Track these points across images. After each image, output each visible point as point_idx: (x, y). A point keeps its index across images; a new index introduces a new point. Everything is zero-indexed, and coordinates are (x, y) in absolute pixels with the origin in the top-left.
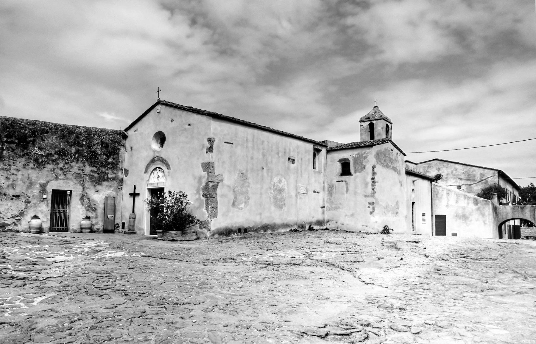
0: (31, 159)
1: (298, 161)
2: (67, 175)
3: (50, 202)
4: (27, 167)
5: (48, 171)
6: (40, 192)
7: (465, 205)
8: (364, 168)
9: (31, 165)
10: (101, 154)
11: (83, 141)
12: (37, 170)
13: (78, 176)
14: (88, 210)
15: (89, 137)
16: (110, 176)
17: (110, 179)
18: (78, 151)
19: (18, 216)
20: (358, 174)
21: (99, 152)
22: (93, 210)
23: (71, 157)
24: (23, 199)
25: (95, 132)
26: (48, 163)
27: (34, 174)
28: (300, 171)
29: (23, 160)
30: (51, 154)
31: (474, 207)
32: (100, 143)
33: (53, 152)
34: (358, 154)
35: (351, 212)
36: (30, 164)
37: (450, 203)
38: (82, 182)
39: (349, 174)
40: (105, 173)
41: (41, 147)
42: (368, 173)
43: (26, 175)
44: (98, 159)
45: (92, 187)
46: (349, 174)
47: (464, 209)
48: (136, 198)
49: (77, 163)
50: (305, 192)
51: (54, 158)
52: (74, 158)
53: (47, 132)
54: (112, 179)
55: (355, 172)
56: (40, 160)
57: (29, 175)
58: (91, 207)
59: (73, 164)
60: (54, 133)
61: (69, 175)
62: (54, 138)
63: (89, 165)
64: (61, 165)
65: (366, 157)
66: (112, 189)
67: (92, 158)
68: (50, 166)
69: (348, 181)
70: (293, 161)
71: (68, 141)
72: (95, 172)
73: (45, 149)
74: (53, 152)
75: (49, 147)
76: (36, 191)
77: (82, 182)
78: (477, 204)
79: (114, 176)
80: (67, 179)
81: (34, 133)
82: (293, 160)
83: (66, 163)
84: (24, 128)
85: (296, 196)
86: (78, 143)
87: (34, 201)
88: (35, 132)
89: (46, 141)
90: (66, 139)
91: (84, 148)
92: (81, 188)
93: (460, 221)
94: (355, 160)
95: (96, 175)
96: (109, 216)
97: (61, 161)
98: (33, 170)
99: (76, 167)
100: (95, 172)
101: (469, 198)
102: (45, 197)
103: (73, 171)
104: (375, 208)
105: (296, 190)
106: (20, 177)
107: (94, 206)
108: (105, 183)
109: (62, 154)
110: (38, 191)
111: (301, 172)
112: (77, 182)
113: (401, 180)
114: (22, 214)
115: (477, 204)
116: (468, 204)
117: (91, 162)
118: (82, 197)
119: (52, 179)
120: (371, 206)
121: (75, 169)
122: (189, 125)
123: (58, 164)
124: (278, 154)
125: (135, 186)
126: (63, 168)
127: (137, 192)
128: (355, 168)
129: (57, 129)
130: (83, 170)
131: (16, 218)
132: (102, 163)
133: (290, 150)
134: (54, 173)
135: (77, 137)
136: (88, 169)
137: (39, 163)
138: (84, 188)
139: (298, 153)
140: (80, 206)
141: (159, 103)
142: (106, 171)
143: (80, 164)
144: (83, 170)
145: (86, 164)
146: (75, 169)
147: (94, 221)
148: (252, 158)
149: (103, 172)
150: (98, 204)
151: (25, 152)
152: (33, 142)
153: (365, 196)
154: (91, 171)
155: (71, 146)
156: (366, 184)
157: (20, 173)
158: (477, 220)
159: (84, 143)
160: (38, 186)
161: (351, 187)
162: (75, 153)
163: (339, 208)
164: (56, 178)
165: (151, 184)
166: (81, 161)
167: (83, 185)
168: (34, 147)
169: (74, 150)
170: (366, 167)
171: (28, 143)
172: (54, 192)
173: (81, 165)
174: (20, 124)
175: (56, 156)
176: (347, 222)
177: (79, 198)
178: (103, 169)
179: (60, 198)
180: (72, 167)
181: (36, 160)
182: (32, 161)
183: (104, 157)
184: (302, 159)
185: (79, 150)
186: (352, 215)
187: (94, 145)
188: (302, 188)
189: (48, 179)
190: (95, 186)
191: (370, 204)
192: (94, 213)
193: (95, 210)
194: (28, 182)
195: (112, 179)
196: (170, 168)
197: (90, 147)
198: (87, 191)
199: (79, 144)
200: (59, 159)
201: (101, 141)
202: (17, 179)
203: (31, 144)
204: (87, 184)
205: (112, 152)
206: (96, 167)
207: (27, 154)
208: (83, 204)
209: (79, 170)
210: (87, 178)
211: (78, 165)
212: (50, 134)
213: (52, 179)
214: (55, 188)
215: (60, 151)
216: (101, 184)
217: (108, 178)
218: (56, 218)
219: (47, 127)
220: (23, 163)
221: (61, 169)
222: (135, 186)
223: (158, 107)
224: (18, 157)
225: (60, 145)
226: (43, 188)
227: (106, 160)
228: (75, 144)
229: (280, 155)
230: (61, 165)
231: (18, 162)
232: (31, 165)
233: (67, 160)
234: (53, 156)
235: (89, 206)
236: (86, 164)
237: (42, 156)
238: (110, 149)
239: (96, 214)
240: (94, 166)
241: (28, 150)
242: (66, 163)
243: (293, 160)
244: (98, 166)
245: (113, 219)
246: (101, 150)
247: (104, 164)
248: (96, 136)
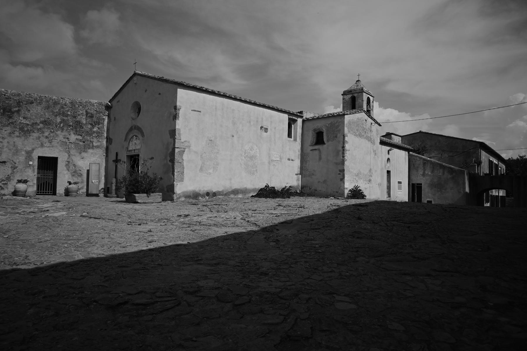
0: (16, 128)
1: (271, 130)
2: (53, 143)
3: (36, 167)
4: (13, 135)
5: (33, 139)
6: (26, 158)
8: (336, 137)
9: (17, 133)
10: (86, 124)
11: (68, 111)
12: (23, 138)
13: (64, 144)
14: (73, 176)
15: (74, 108)
16: (95, 144)
17: (95, 147)
18: (63, 121)
19: (4, 181)
20: (330, 142)
21: (84, 122)
22: (79, 176)
23: (56, 126)
24: (9, 165)
25: (80, 103)
26: (34, 132)
27: (19, 142)
28: (273, 139)
29: (9, 129)
30: (36, 123)
31: (450, 176)
32: (85, 113)
33: (38, 122)
34: (331, 123)
36: (15, 132)
38: (67, 149)
39: (323, 143)
40: (90, 141)
41: (26, 116)
42: (339, 142)
43: (12, 143)
44: (83, 128)
45: (78, 154)
46: (323, 143)
49: (62, 132)
50: (278, 159)
51: (39, 127)
52: (59, 127)
53: (32, 103)
54: (97, 147)
55: (328, 141)
56: (26, 129)
57: (14, 142)
58: (76, 173)
59: (59, 132)
60: (40, 103)
61: (55, 143)
62: (39, 108)
63: (74, 134)
64: (46, 134)
65: (338, 126)
66: (97, 156)
67: (77, 127)
68: (35, 135)
70: (266, 130)
71: (52, 111)
72: (80, 140)
73: (30, 118)
74: (38, 122)
75: (34, 117)
76: (22, 158)
77: (67, 149)
79: (99, 144)
80: (52, 147)
81: (19, 103)
82: (267, 129)
83: (51, 132)
84: (8, 98)
85: (269, 163)
86: (63, 113)
87: (20, 167)
88: (19, 102)
89: (31, 111)
90: (51, 109)
91: (69, 118)
92: (67, 155)
95: (81, 143)
96: (93, 181)
97: (46, 130)
98: (19, 138)
99: (61, 135)
100: (80, 140)
102: (31, 163)
103: (59, 139)
104: (346, 175)
105: (269, 157)
106: (6, 144)
107: (80, 172)
108: (90, 151)
109: (46, 123)
110: (24, 158)
111: (275, 140)
112: (62, 150)
113: (375, 149)
114: (8, 178)
116: (444, 173)
117: (76, 131)
118: (68, 164)
119: (38, 146)
120: (341, 173)
121: (61, 137)
122: (160, 94)
123: (43, 132)
124: (250, 122)
125: (117, 153)
126: (49, 136)
127: (119, 158)
129: (42, 100)
130: (68, 138)
131: (3, 183)
132: (87, 132)
133: (262, 119)
134: (40, 141)
135: (63, 108)
136: (73, 137)
137: (25, 131)
138: (69, 155)
139: (271, 122)
140: (66, 172)
141: (135, 74)
142: (92, 140)
143: (65, 133)
144: (68, 138)
145: (72, 133)
146: (61, 137)
147: (80, 186)
148: (221, 126)
149: (88, 140)
150: (84, 169)
151: (11, 121)
152: (18, 111)
154: (77, 139)
155: (56, 116)
156: (338, 152)
157: (6, 140)
159: (69, 113)
160: (23, 153)
162: (61, 123)
163: (313, 174)
164: (42, 145)
166: (67, 130)
167: (68, 153)
168: (19, 116)
169: (59, 120)
171: (13, 113)
172: (39, 158)
173: (66, 134)
174: (5, 95)
175: (41, 125)
177: (64, 164)
178: (89, 138)
179: (48, 165)
180: (57, 135)
181: (22, 129)
182: (18, 130)
183: (90, 126)
184: (275, 128)
185: (64, 120)
186: (325, 182)
187: (79, 115)
188: (275, 156)
189: (33, 146)
190: (80, 153)
191: (340, 171)
192: (80, 179)
193: (81, 175)
194: (14, 148)
195: (97, 147)
197: (75, 117)
198: (74, 158)
199: (64, 114)
200: (44, 128)
201: (86, 111)
202: (3, 146)
203: (15, 114)
204: (73, 152)
205: (97, 122)
206: (81, 135)
207: (12, 123)
208: (68, 170)
209: (64, 138)
210: (73, 146)
211: (63, 134)
212: (34, 104)
213: (38, 146)
214: (41, 155)
215: (45, 121)
216: (86, 152)
217: (93, 146)
218: (44, 183)
219: (32, 98)
220: (8, 131)
221: (47, 137)
223: (135, 78)
224: (3, 126)
225: (45, 114)
226: (29, 154)
227: (91, 129)
228: (60, 114)
229: (252, 123)
230: (46, 134)
231: (4, 131)
232: (17, 133)
233: (53, 129)
234: (39, 125)
235: (75, 172)
236: (72, 133)
237: (28, 125)
238: (95, 119)
239: (82, 180)
240: (79, 135)
241: (13, 119)
242: (51, 132)
243: (267, 129)
244: (83, 134)
245: (97, 183)
246: (86, 120)
247: (90, 133)
248: (81, 107)
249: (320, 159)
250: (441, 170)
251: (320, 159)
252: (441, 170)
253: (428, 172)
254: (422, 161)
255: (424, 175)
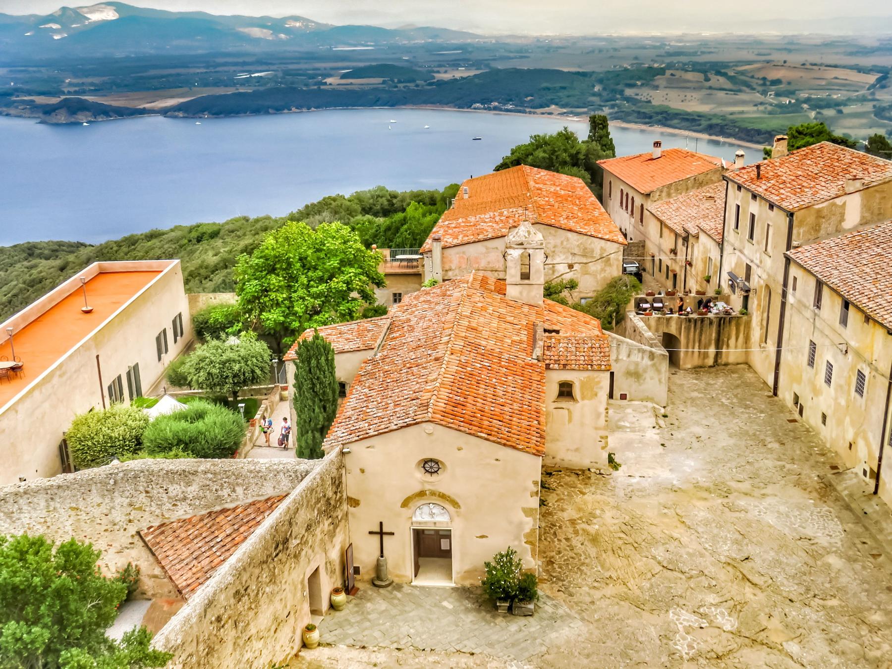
7: (639, 360)
8: (596, 395)
20: (586, 402)
35: (576, 447)
37: (620, 357)
47: (637, 364)
48: (385, 537)
55: (583, 398)
65: (599, 382)
69: (571, 408)
78: (653, 359)
93: (631, 380)
94: (583, 385)
101: (644, 351)
115: (653, 359)
116: (643, 358)
125: (381, 523)
128: (583, 394)
153: (596, 428)
156: (598, 415)
158: (652, 378)
161: (576, 415)
163: (558, 440)
165: (420, 523)
170: (599, 395)
176: (570, 458)
196: (459, 506)
222: (381, 523)
249: (570, 420)
250: (640, 354)
251: (570, 420)
252: (640, 354)
253: (623, 356)
254: (615, 342)
255: (617, 360)
